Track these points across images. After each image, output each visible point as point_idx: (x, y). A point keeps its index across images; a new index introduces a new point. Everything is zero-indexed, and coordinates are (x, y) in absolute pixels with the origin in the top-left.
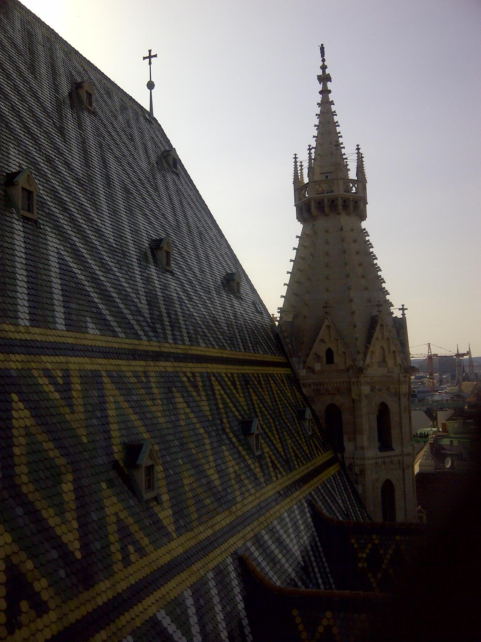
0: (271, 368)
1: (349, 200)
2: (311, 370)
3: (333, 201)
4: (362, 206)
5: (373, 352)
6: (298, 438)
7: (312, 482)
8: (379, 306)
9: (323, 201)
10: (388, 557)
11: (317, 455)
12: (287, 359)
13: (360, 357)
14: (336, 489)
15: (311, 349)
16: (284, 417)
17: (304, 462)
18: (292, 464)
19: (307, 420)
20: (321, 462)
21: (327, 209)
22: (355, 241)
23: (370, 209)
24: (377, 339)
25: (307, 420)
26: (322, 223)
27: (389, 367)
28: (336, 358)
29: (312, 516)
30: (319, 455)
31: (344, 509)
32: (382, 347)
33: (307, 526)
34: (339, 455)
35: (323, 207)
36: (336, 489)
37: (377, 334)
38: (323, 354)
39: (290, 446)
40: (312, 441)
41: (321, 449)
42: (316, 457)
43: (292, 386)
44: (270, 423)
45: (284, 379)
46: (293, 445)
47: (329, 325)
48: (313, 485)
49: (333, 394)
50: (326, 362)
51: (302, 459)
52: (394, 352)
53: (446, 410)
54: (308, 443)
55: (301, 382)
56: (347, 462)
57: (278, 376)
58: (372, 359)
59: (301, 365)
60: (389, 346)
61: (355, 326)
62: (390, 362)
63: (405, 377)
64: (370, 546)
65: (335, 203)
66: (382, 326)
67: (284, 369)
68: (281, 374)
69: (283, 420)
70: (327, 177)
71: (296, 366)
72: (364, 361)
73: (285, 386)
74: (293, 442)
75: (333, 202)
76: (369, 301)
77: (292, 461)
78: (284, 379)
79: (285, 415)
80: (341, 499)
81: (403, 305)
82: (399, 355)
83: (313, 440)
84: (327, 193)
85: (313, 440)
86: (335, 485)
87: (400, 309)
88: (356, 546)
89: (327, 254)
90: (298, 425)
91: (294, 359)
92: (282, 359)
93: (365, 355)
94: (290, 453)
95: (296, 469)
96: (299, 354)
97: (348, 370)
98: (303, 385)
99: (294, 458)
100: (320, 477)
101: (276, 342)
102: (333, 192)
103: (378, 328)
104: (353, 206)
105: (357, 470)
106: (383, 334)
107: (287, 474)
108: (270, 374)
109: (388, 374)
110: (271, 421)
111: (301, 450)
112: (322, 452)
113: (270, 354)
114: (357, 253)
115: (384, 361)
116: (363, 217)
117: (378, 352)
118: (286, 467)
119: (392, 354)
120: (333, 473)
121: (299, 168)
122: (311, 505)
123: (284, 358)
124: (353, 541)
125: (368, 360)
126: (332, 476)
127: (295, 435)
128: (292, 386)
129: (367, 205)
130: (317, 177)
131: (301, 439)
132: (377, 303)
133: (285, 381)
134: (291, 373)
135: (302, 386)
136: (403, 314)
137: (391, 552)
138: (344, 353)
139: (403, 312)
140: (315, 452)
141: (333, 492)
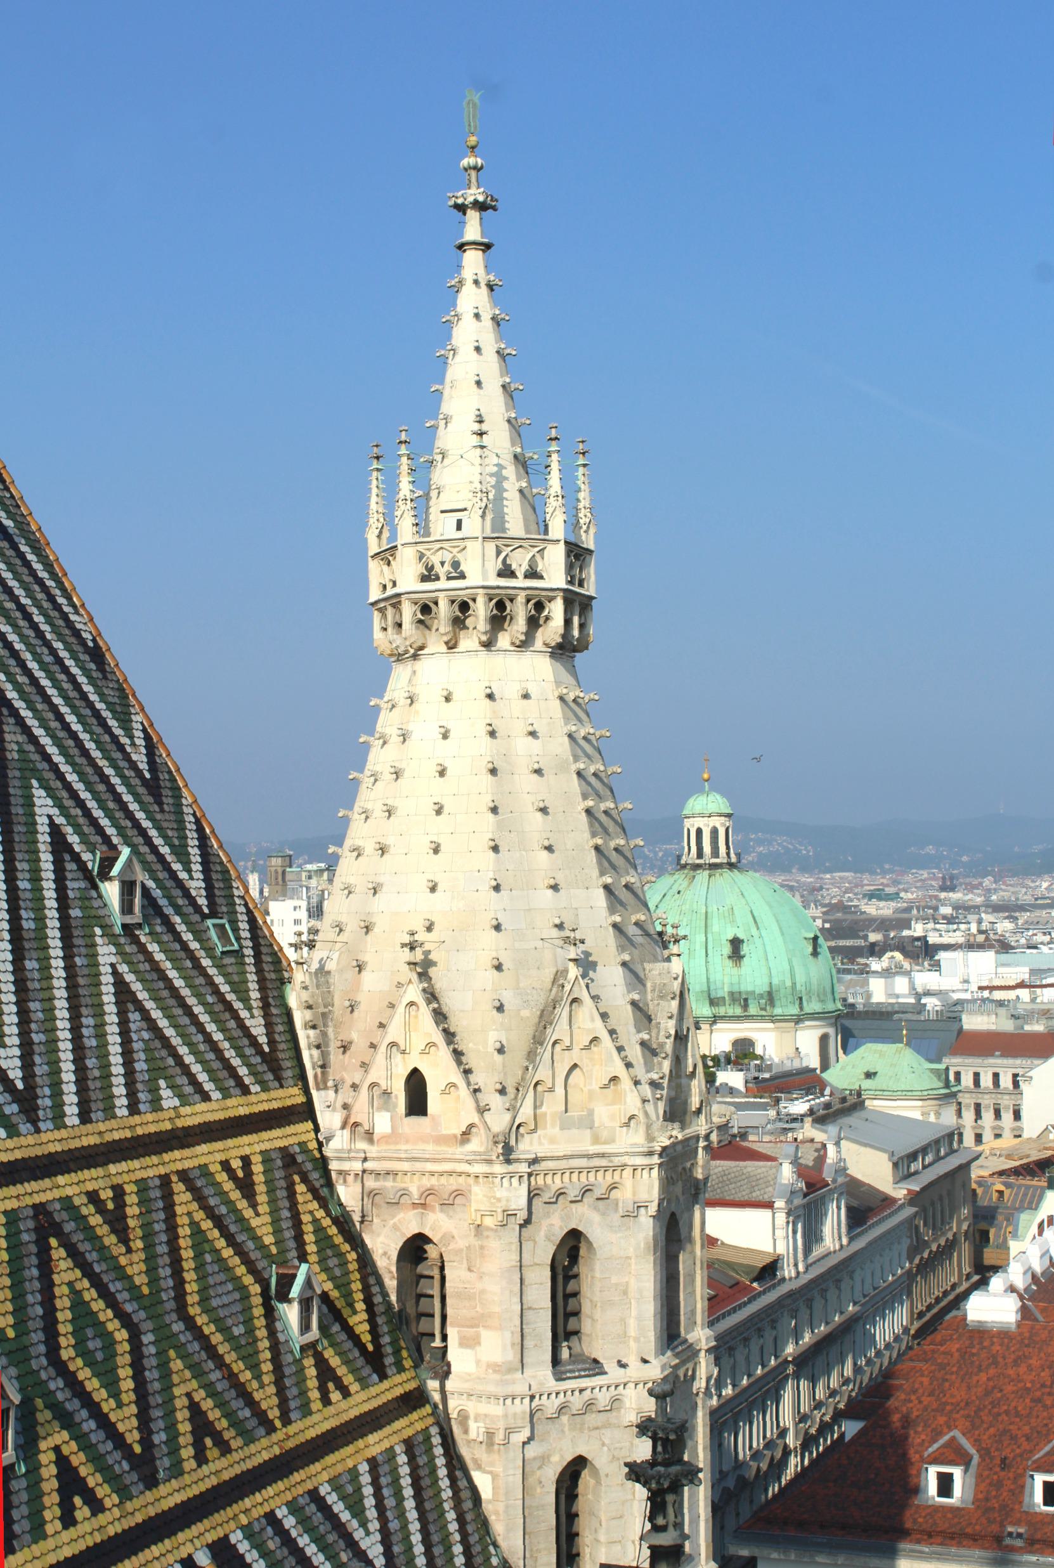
0: (204, 1148)
9: (436, 603)
11: (316, 1405)
12: (307, 1091)
15: (364, 1066)
17: (234, 1444)
20: (327, 1426)
25: (296, 1306)
27: (596, 1125)
30: (326, 1401)
34: (433, 1385)
39: (181, 1403)
40: (309, 1362)
41: (348, 1379)
44: (109, 1343)
48: (246, 1511)
49: (424, 1205)
55: (333, 1166)
56: (454, 1405)
74: (209, 1388)
78: (257, 1168)
79: (204, 1301)
80: (385, 1532)
86: (368, 1491)
91: (323, 1093)
95: (177, 1471)
97: (466, 1135)
98: (340, 1172)
101: (272, 1042)
105: (476, 1430)
108: (183, 1175)
110: (122, 1335)
112: (354, 1387)
113: (216, 1095)
123: (295, 1091)
126: (373, 1463)
135: (334, 1175)
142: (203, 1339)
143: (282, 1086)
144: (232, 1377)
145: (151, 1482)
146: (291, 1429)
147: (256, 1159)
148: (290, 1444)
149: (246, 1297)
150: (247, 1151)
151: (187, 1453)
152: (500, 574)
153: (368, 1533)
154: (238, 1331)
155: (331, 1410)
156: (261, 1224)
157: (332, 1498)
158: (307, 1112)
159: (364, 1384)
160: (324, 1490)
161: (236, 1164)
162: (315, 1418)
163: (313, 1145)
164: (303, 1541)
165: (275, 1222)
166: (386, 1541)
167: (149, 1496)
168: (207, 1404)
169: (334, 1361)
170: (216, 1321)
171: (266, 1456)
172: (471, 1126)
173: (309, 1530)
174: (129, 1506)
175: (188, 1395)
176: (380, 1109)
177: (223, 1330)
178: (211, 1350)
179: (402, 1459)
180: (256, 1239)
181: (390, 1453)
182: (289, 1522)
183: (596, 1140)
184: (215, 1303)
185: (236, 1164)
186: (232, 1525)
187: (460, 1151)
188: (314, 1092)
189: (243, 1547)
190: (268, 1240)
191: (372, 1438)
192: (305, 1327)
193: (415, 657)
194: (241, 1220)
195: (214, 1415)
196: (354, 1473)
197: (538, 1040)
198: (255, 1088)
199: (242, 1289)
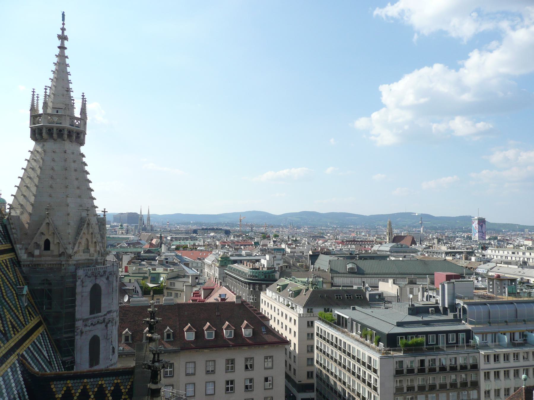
1: (72, 131)
2: (31, 254)
3: (60, 131)
4: (82, 136)
5: (80, 243)
6: (16, 311)
7: (24, 344)
8: (88, 210)
9: (53, 129)
10: (77, 394)
11: (30, 321)
12: (12, 245)
13: (70, 246)
14: (43, 344)
15: (33, 239)
16: (5, 297)
17: (19, 330)
18: (9, 335)
19: (25, 296)
20: (33, 326)
21: (55, 136)
22: (74, 162)
23: (88, 138)
24: (84, 233)
25: (25, 296)
26: (50, 145)
28: (52, 247)
29: (22, 373)
30: (31, 320)
31: (47, 358)
32: (87, 239)
33: (17, 382)
35: (52, 134)
36: (43, 344)
37: (84, 230)
38: (42, 244)
39: (8, 320)
40: (26, 310)
41: (33, 314)
42: (29, 323)
43: (14, 268)
45: (8, 263)
46: (11, 318)
47: (49, 222)
50: (43, 249)
51: (18, 328)
52: (95, 243)
53: (129, 255)
54: (24, 312)
55: (22, 263)
57: (3, 262)
58: (79, 247)
59: (23, 251)
60: (92, 238)
61: (69, 224)
62: (92, 250)
63: (101, 259)
64: (65, 389)
65: (62, 132)
66: (88, 224)
67: (8, 255)
68: (5, 260)
69: (5, 299)
70: (57, 112)
71: (19, 251)
72: (73, 249)
73: (8, 269)
74: (11, 316)
75: (60, 131)
76: (81, 206)
77: (10, 332)
78: (8, 263)
80: (46, 350)
81: (105, 209)
82: (99, 245)
83: (27, 309)
84: (56, 124)
85: (27, 309)
86: (42, 341)
87: (102, 211)
88: (54, 390)
89: (53, 169)
90: (17, 300)
91: (18, 246)
92: (7, 246)
93: (75, 244)
94: (8, 326)
95: (12, 338)
96: (23, 242)
97: (60, 255)
98: (24, 266)
99: (11, 329)
100: (31, 338)
101: (4, 232)
102: (61, 124)
103: (85, 226)
104: (76, 136)
106: (88, 230)
107: (4, 344)
109: (90, 258)
111: (17, 320)
112: (35, 316)
114: (76, 170)
115: (88, 248)
116: (82, 143)
117: (84, 242)
118: (4, 339)
119: (94, 244)
120: (41, 332)
121: (36, 98)
122: (22, 364)
123: (10, 245)
124: (52, 386)
125: (76, 249)
126: (41, 334)
127: (14, 309)
128: (14, 268)
129: (86, 135)
130: (49, 111)
131: (18, 311)
132: (87, 208)
133: (9, 265)
134: (15, 256)
135: (22, 266)
136: (104, 215)
137: (79, 391)
138: (59, 243)
139: (104, 213)
140: (29, 318)
141: (40, 347)
142: (8, 304)
143: (8, 243)
144: (15, 314)
145: (8, 341)
146: (28, 326)
147: (7, 260)
148: (29, 330)
149: (13, 294)
150: (5, 258)
151: (12, 332)
152: (70, 125)
153: (44, 351)
154: (14, 302)
155: (32, 322)
156: (11, 276)
157: (37, 343)
158: (13, 250)
159: (36, 316)
160: (36, 341)
161: (4, 261)
162: (30, 323)
163: (16, 258)
164: (35, 353)
165: (14, 276)
166: (47, 353)
167: (8, 343)
168: (12, 320)
169: (30, 310)
170: (9, 300)
171: (25, 333)
172: (63, 252)
173: (35, 351)
174: (6, 346)
175: (9, 318)
176: (36, 249)
177: (11, 302)
178: (10, 306)
179: (45, 333)
180: (12, 280)
181: (43, 331)
182: (32, 349)
183: (90, 256)
184: (9, 295)
185: (4, 261)
186: (23, 350)
187: (58, 259)
188: (14, 246)
189: (26, 355)
190: (14, 280)
191: (40, 328)
192: (26, 302)
193: (45, 141)
194: (8, 275)
195: (14, 323)
196: (39, 336)
197: (78, 234)
198: (4, 243)
199: (12, 292)
